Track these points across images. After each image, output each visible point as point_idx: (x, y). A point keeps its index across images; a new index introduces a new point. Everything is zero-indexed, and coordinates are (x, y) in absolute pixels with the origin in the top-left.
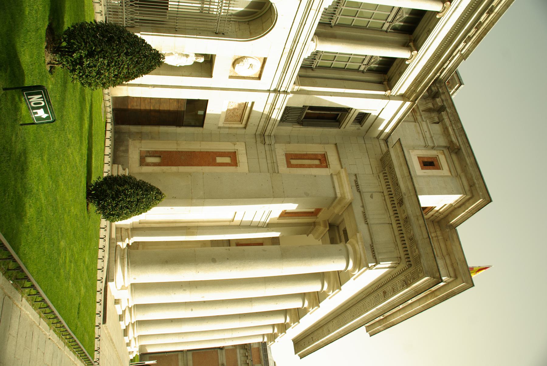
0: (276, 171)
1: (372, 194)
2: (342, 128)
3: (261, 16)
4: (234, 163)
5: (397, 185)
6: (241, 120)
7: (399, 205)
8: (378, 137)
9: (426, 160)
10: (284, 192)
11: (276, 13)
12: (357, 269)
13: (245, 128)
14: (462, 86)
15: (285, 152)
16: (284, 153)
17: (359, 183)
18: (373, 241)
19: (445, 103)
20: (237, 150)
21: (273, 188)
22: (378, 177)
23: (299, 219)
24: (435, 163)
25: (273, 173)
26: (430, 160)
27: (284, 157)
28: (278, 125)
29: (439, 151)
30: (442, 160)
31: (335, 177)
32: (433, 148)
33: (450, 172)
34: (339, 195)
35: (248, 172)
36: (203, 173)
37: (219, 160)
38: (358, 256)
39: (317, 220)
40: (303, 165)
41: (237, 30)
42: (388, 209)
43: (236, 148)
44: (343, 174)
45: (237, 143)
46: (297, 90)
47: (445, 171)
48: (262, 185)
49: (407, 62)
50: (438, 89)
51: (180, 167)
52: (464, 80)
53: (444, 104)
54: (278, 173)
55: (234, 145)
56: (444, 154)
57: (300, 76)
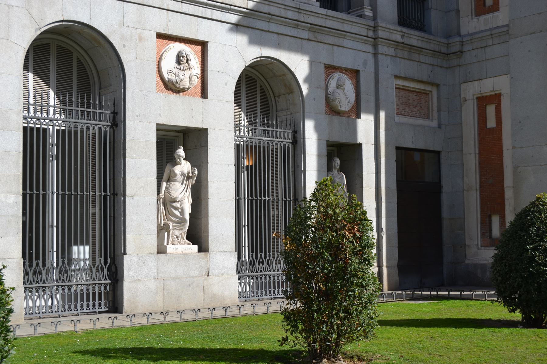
0: (506, 29)
3: (266, 79)
6: (426, 94)
11: (259, 59)
13: (438, 86)
15: (474, 16)
16: (475, 20)
20: (473, 95)
27: (482, 18)
28: (430, 33)
37: (491, 123)
41: (289, 113)
43: (471, 98)
45: (462, 96)
46: (371, 10)
54: (507, 26)
55: (466, 100)
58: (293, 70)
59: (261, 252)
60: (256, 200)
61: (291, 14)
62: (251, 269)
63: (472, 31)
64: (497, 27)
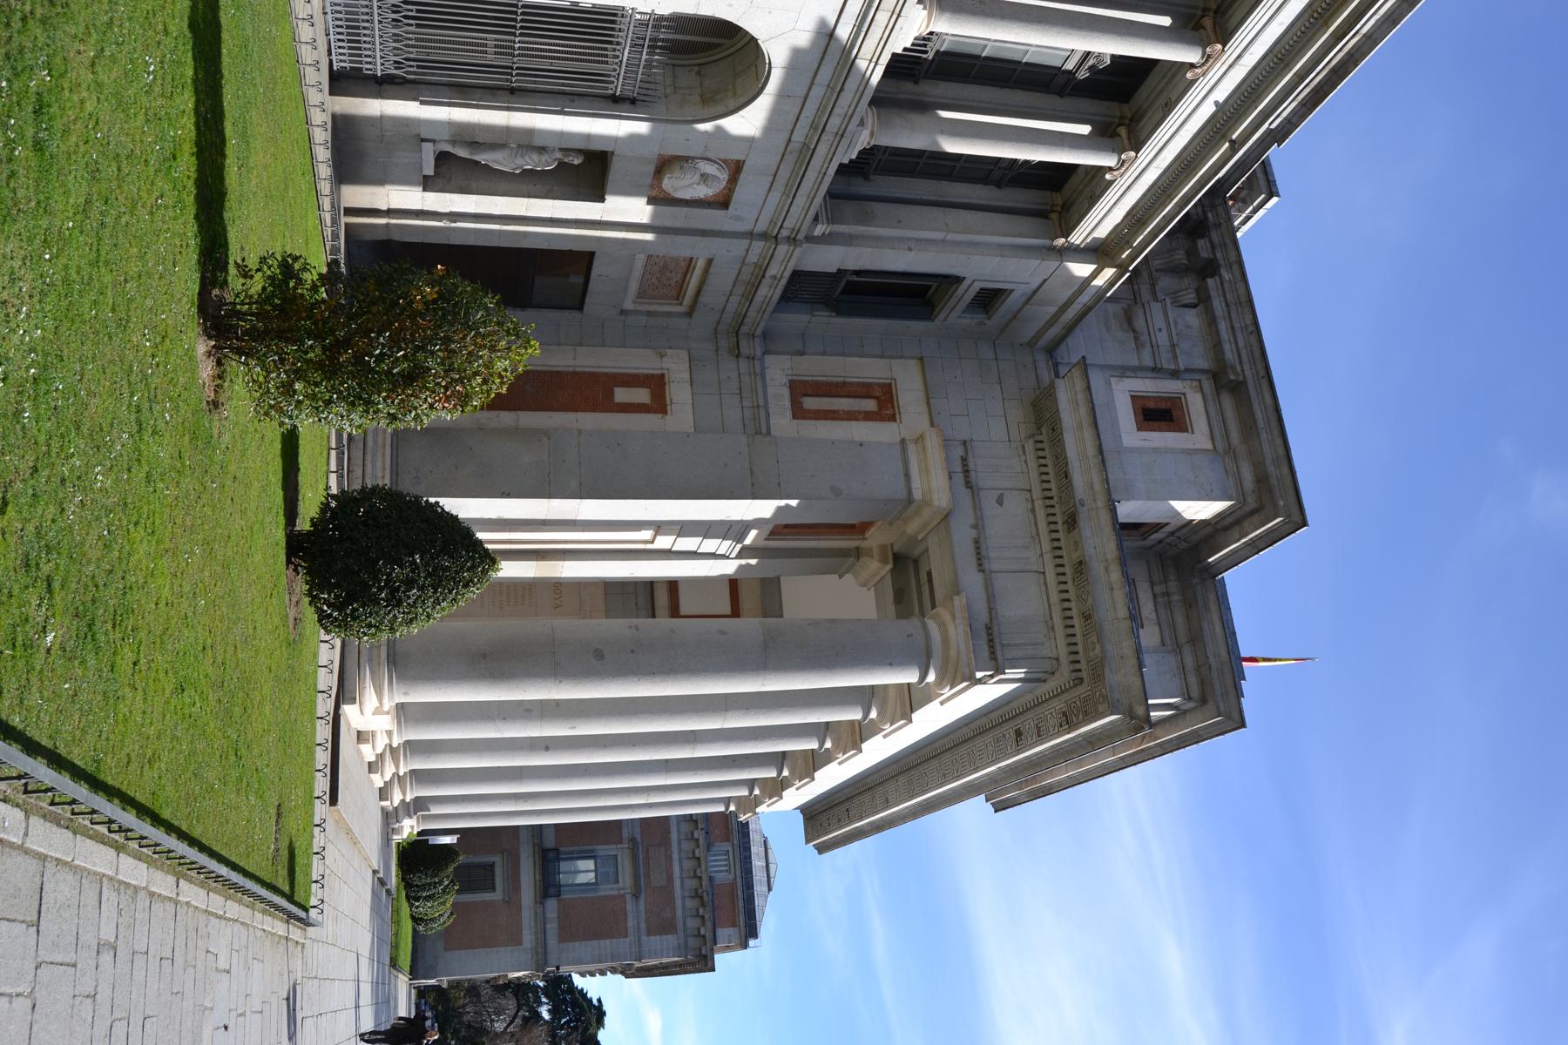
0: (764, 430)
1: (1002, 495)
2: (937, 322)
3: (732, 54)
4: (659, 405)
5: (1066, 476)
6: (679, 296)
7: (1066, 526)
8: (1031, 344)
9: (1152, 405)
10: (779, 485)
11: (767, 61)
12: (947, 685)
13: (689, 314)
14: (1275, 200)
15: (790, 378)
16: (785, 380)
17: (971, 466)
18: (994, 615)
19: (1219, 255)
20: (668, 369)
21: (752, 474)
22: (1021, 452)
23: (819, 539)
24: (1175, 413)
25: (757, 433)
26: (1163, 406)
27: (786, 392)
28: (775, 310)
29: (1188, 382)
30: (1196, 405)
31: (911, 448)
32: (1175, 374)
33: (1212, 438)
34: (917, 495)
35: (693, 429)
36: (580, 432)
37: (622, 395)
38: (953, 653)
39: (864, 544)
40: (834, 412)
41: (668, 90)
42: (1038, 534)
43: (665, 365)
44: (933, 443)
45: (669, 352)
46: (824, 234)
47: (1199, 437)
48: (726, 465)
49: (1108, 177)
50: (1205, 213)
51: (521, 413)
52: (1281, 184)
53: (1215, 255)
54: (769, 433)
55: (661, 357)
56: (1202, 391)
57: (832, 195)
58: (741, 113)
59: (418, 67)
60: (514, 34)
61: (835, 122)
62: (385, 6)
63: (769, 374)
64: (768, 415)
